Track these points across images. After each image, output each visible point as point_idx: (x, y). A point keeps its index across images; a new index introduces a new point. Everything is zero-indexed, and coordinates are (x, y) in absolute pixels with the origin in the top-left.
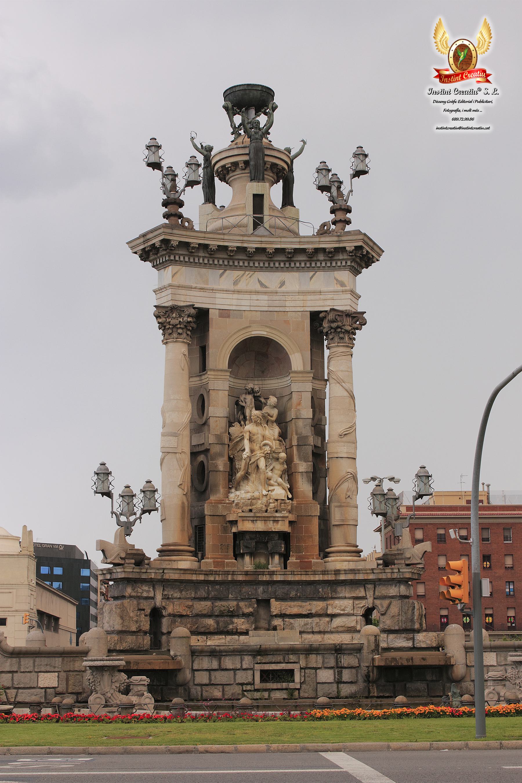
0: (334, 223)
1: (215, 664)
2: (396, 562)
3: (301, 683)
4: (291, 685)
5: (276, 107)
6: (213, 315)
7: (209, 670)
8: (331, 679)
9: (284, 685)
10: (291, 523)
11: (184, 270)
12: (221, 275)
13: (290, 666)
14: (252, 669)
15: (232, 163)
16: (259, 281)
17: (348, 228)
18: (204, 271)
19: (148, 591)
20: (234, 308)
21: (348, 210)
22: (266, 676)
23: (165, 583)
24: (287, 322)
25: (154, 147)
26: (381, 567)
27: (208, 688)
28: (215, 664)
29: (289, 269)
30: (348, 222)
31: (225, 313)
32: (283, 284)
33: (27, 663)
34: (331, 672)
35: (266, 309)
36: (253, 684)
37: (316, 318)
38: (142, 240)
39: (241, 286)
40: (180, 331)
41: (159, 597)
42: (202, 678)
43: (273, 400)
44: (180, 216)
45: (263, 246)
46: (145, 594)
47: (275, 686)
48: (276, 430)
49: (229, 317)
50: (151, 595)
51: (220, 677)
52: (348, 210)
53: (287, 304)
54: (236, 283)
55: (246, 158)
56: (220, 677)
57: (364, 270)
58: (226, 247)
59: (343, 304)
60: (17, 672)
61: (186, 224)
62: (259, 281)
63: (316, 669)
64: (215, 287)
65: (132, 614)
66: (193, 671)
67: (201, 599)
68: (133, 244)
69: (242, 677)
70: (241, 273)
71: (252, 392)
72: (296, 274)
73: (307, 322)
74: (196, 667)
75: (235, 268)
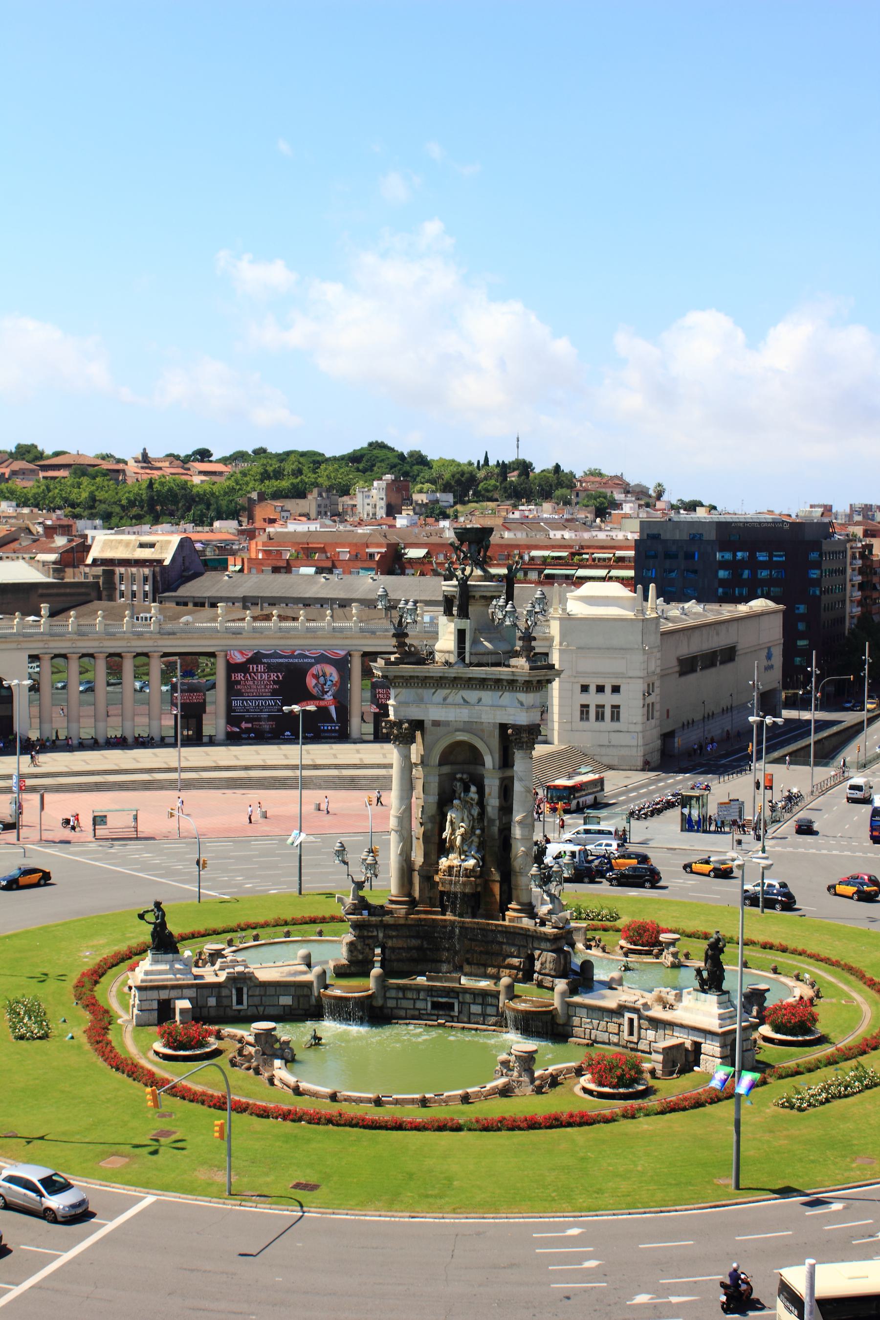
1: (401, 995)
3: (460, 1012)
4: (452, 1014)
6: (427, 725)
7: (397, 999)
8: (480, 1012)
9: (447, 1013)
11: (404, 691)
12: (434, 693)
13: (451, 1000)
14: (426, 1000)
16: (463, 698)
18: (420, 691)
19: (372, 932)
20: (442, 719)
22: (435, 1005)
23: (386, 927)
24: (483, 731)
27: (396, 1011)
28: (401, 995)
29: (483, 689)
31: (436, 723)
32: (480, 700)
33: (271, 991)
34: (480, 1007)
35: (467, 719)
39: (449, 700)
41: (381, 935)
42: (391, 1003)
43: (473, 789)
44: (406, 644)
45: (460, 675)
46: (370, 934)
47: (441, 1013)
48: (475, 811)
49: (439, 725)
50: (375, 934)
51: (405, 1004)
53: (483, 716)
54: (445, 699)
56: (405, 1004)
59: (522, 718)
60: (265, 995)
61: (413, 649)
62: (463, 698)
63: (469, 1004)
65: (359, 948)
66: (385, 998)
67: (413, 937)
69: (420, 1005)
70: (448, 691)
71: (461, 780)
72: (489, 693)
74: (388, 995)
75: (445, 688)
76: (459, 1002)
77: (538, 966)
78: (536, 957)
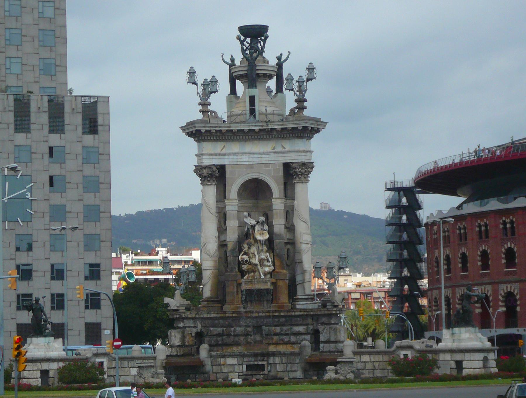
0: (296, 108)
2: (328, 304)
5: (268, 37)
10: (273, 284)
15: (240, 75)
17: (306, 113)
21: (306, 101)
25: (192, 73)
26: (320, 307)
30: (305, 108)
36: (243, 372)
37: (287, 166)
38: (186, 128)
40: (209, 179)
52: (306, 101)
55: (246, 72)
57: (316, 135)
58: (232, 130)
64: (228, 152)
68: (184, 128)
73: (281, 169)
76: (268, 364)
77: (322, 338)
78: (320, 330)
